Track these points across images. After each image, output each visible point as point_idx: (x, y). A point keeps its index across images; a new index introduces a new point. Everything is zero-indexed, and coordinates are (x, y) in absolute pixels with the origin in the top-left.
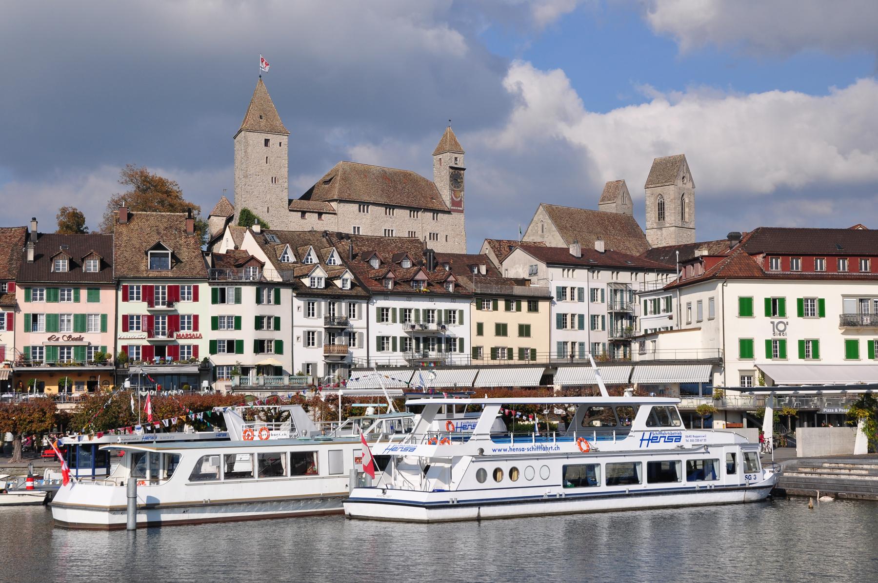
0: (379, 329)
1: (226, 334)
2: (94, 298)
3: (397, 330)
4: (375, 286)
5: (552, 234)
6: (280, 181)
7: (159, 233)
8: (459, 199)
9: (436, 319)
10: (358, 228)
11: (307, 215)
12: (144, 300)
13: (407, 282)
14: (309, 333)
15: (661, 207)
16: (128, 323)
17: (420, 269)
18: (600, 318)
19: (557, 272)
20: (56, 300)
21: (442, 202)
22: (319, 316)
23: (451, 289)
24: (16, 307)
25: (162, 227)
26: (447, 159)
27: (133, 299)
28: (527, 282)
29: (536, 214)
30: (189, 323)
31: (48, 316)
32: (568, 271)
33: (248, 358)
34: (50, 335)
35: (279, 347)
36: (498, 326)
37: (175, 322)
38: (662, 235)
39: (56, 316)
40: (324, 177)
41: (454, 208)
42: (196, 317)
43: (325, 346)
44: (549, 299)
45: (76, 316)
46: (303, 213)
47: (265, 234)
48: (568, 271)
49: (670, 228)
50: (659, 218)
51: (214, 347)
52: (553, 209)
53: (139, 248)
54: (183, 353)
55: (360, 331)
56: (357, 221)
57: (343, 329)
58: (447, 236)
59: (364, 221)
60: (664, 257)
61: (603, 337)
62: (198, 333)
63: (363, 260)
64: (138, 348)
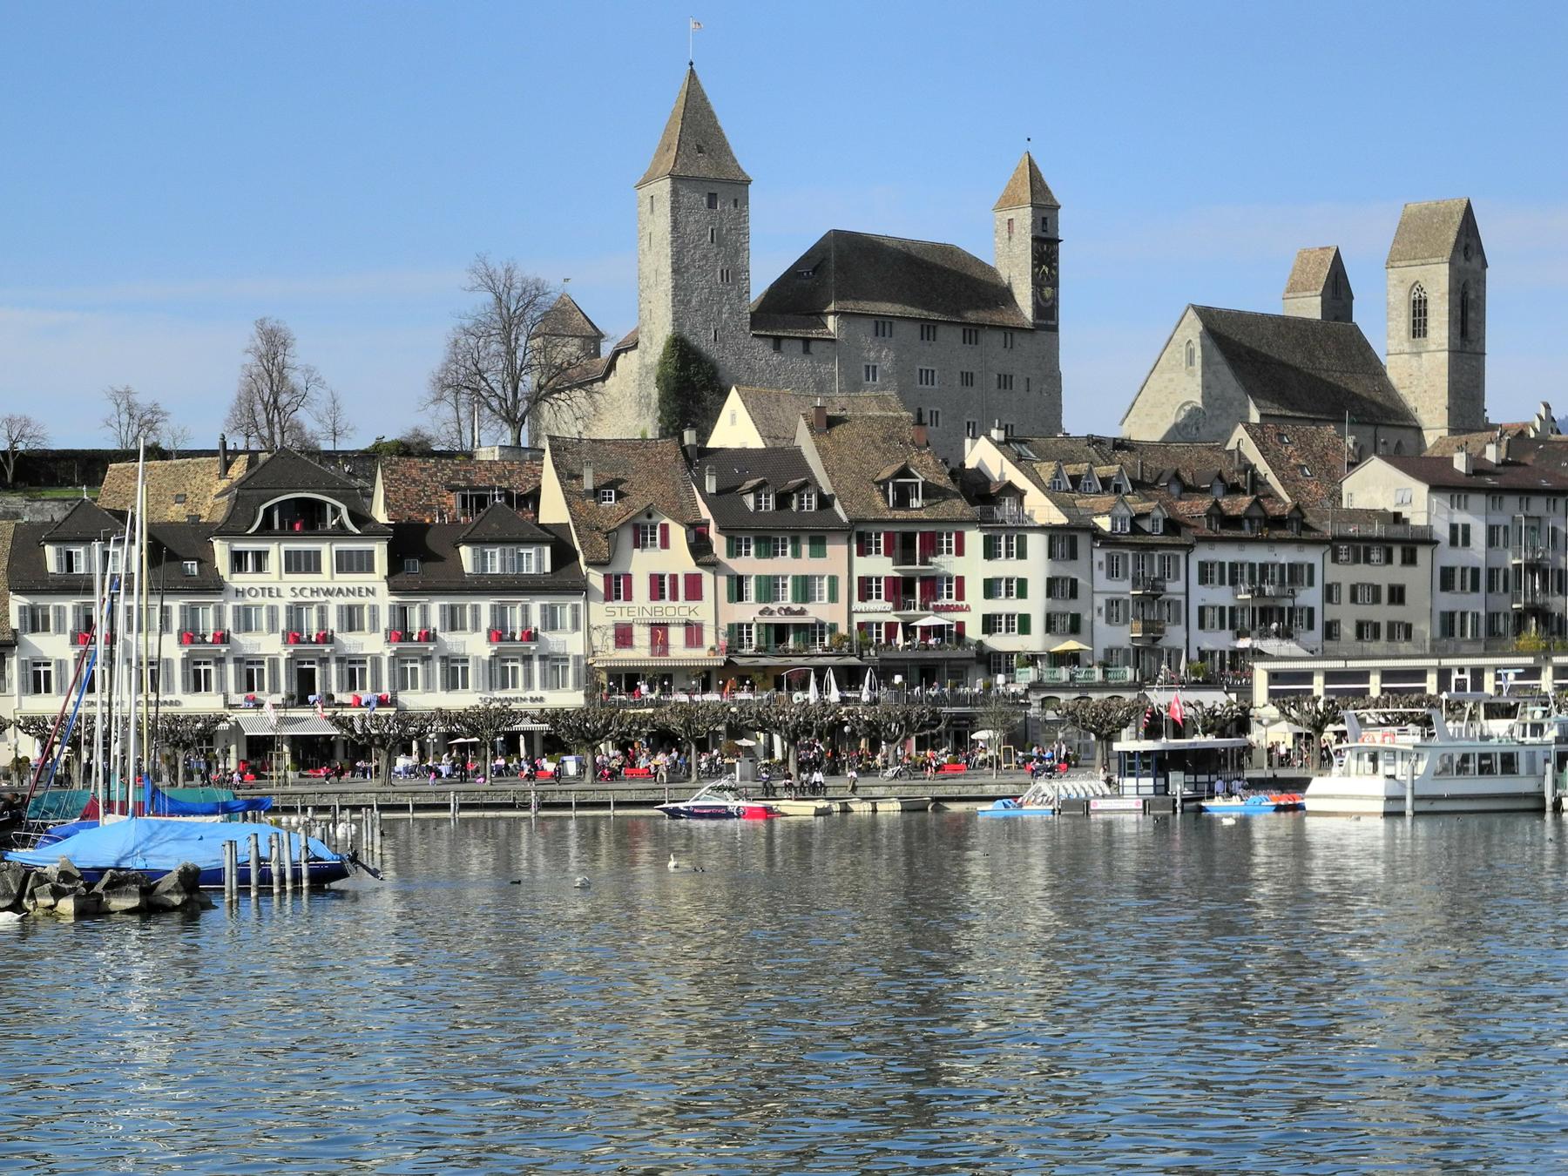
3: (1222, 596)
7: (878, 448)
9: (1277, 578)
12: (887, 554)
15: (1419, 311)
16: (866, 588)
24: (714, 566)
25: (878, 435)
31: (759, 578)
33: (1036, 641)
34: (762, 606)
37: (932, 586)
38: (1421, 366)
39: (768, 577)
42: (960, 580)
45: (795, 578)
49: (1438, 354)
51: (990, 623)
52: (1211, 316)
53: (860, 472)
55: (1177, 598)
56: (872, 354)
57: (1155, 597)
62: (964, 603)
64: (879, 625)
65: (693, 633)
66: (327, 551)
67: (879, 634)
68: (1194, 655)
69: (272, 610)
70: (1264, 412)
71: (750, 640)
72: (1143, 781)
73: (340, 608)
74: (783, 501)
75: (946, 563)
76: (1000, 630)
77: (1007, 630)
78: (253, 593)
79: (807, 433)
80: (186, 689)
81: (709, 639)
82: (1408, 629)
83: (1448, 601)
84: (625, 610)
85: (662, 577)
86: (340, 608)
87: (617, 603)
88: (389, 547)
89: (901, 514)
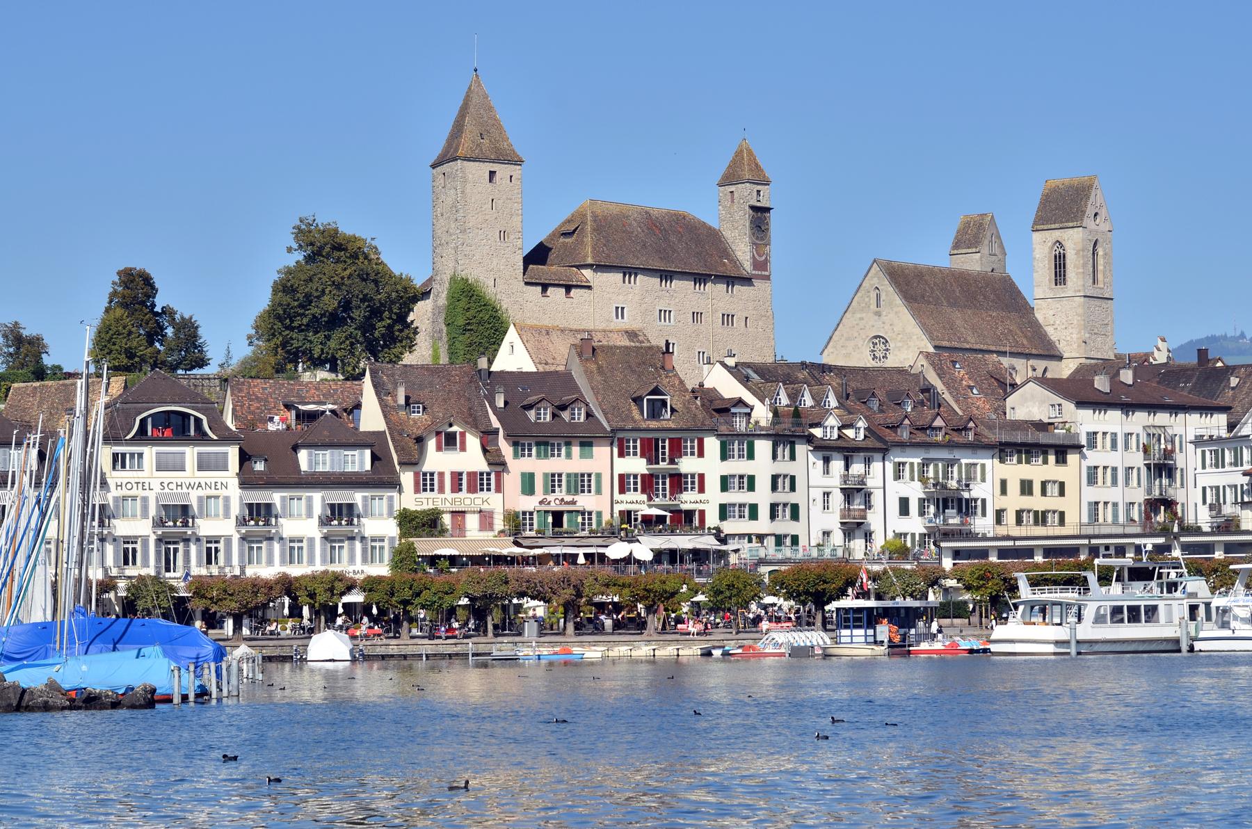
0: (897, 489)
1: (736, 497)
4: (890, 436)
5: (895, 309)
6: (512, 237)
7: (633, 372)
8: (764, 258)
9: (956, 475)
10: (623, 308)
11: (550, 290)
12: (642, 456)
13: (922, 429)
16: (624, 483)
17: (938, 414)
18: (1135, 471)
19: (1086, 414)
20: (546, 456)
21: (735, 262)
23: (971, 437)
24: (504, 464)
26: (746, 193)
27: (629, 455)
28: (1049, 427)
29: (866, 276)
30: (693, 483)
32: (1100, 413)
33: (763, 524)
36: (1023, 482)
37: (678, 482)
40: (561, 227)
41: (757, 272)
42: (702, 477)
44: (1078, 448)
46: (545, 287)
48: (1100, 413)
50: (1056, 280)
56: (621, 297)
58: (747, 318)
59: (630, 297)
60: (1186, 384)
61: (1139, 495)
63: (859, 400)
65: (486, 519)
66: (190, 453)
68: (890, 535)
69: (145, 499)
70: (937, 343)
71: (531, 525)
72: (856, 632)
75: (687, 465)
76: (734, 517)
77: (740, 517)
79: (577, 360)
82: (1062, 515)
83: (1091, 494)
85: (461, 474)
87: (424, 495)
88: (240, 449)
89: (653, 424)
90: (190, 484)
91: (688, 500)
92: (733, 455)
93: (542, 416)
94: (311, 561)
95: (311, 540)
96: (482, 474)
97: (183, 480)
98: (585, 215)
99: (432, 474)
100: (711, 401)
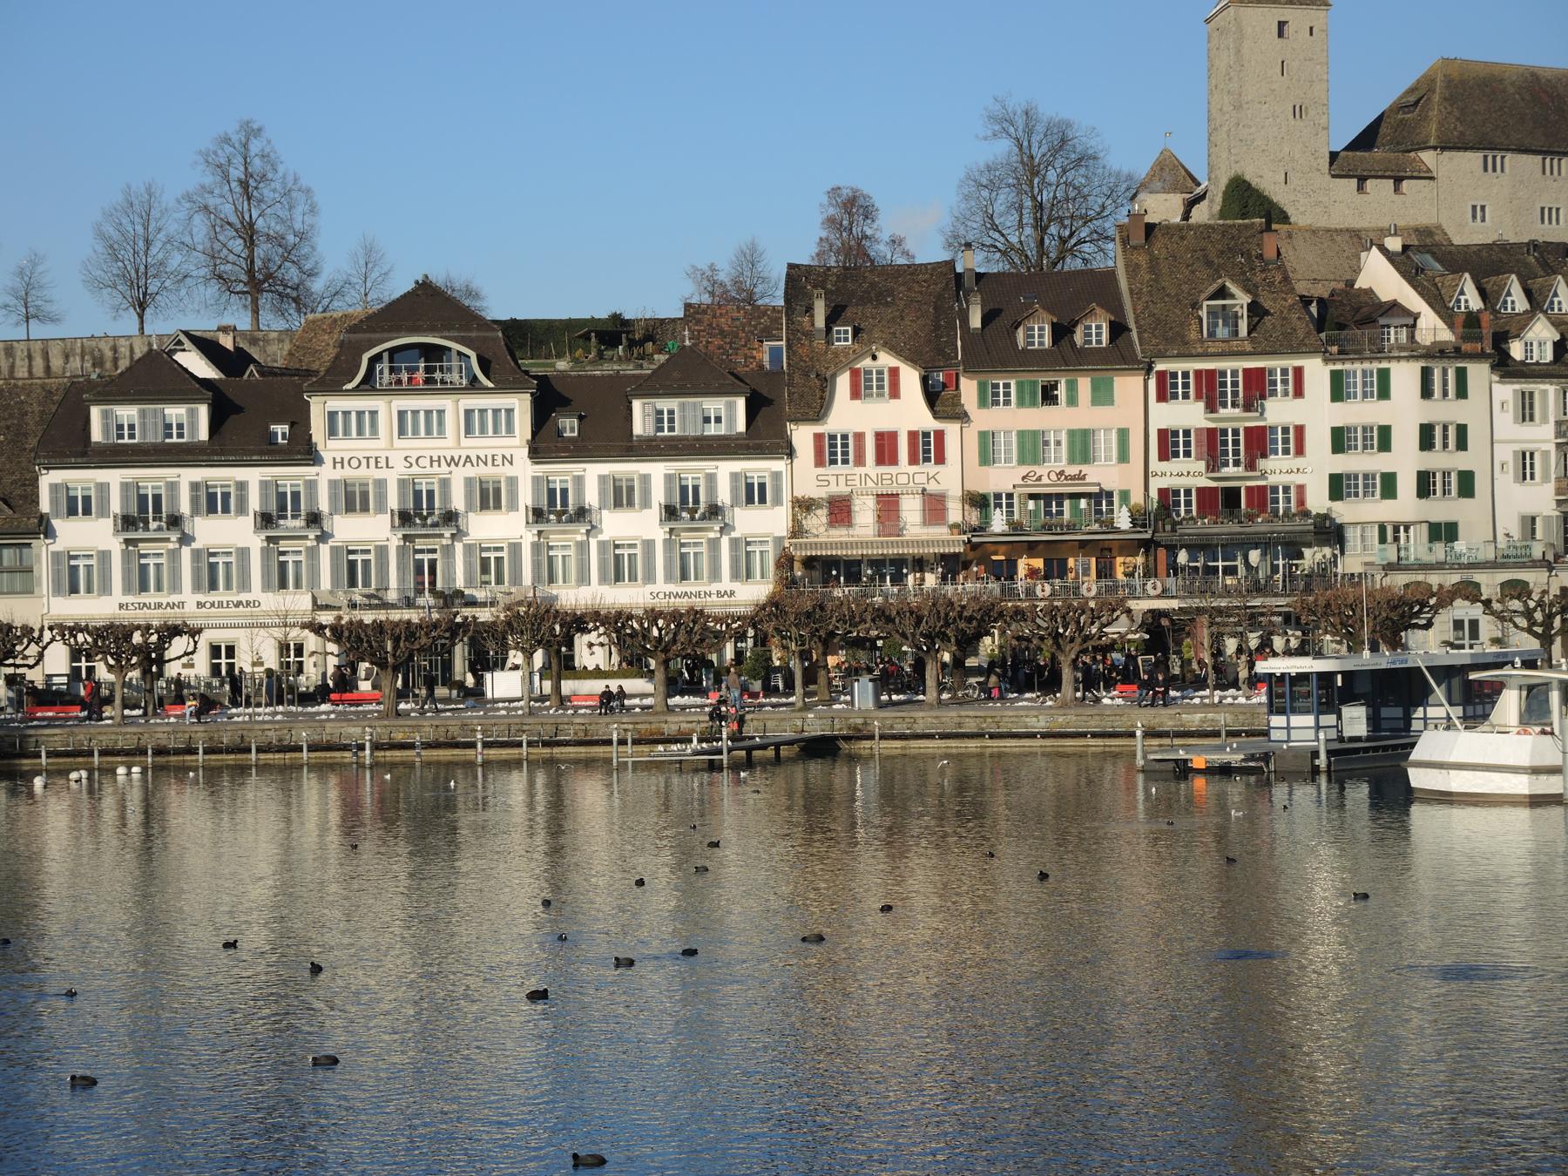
2: (1103, 396)
6: (1312, 113)
7: (1209, 263)
10: (1483, 208)
12: (1198, 397)
14: (1524, 454)
16: (1169, 444)
22: (1545, 420)
24: (962, 416)
30: (1286, 441)
31: (1022, 434)
33: (1406, 505)
34: (1024, 470)
35: (1467, 484)
37: (1259, 443)
39: (1035, 433)
40: (1401, 97)
42: (1300, 430)
43: (1558, 480)
45: (1072, 433)
46: (1362, 180)
47: (1410, 253)
54: (1276, 501)
64: (1188, 492)
65: (934, 506)
66: (453, 407)
67: (1188, 503)
69: (381, 484)
72: (1297, 720)
73: (469, 482)
74: (1061, 332)
75: (1278, 411)
76: (1356, 495)
78: (354, 463)
80: (266, 587)
81: (955, 513)
84: (842, 480)
86: (469, 482)
87: (833, 469)
90: (452, 458)
91: (1278, 469)
92: (1355, 393)
93: (1036, 340)
94: (650, 578)
95: (649, 545)
96: (926, 435)
97: (441, 453)
98: (1433, 81)
99: (845, 437)
100: (1357, 310)
